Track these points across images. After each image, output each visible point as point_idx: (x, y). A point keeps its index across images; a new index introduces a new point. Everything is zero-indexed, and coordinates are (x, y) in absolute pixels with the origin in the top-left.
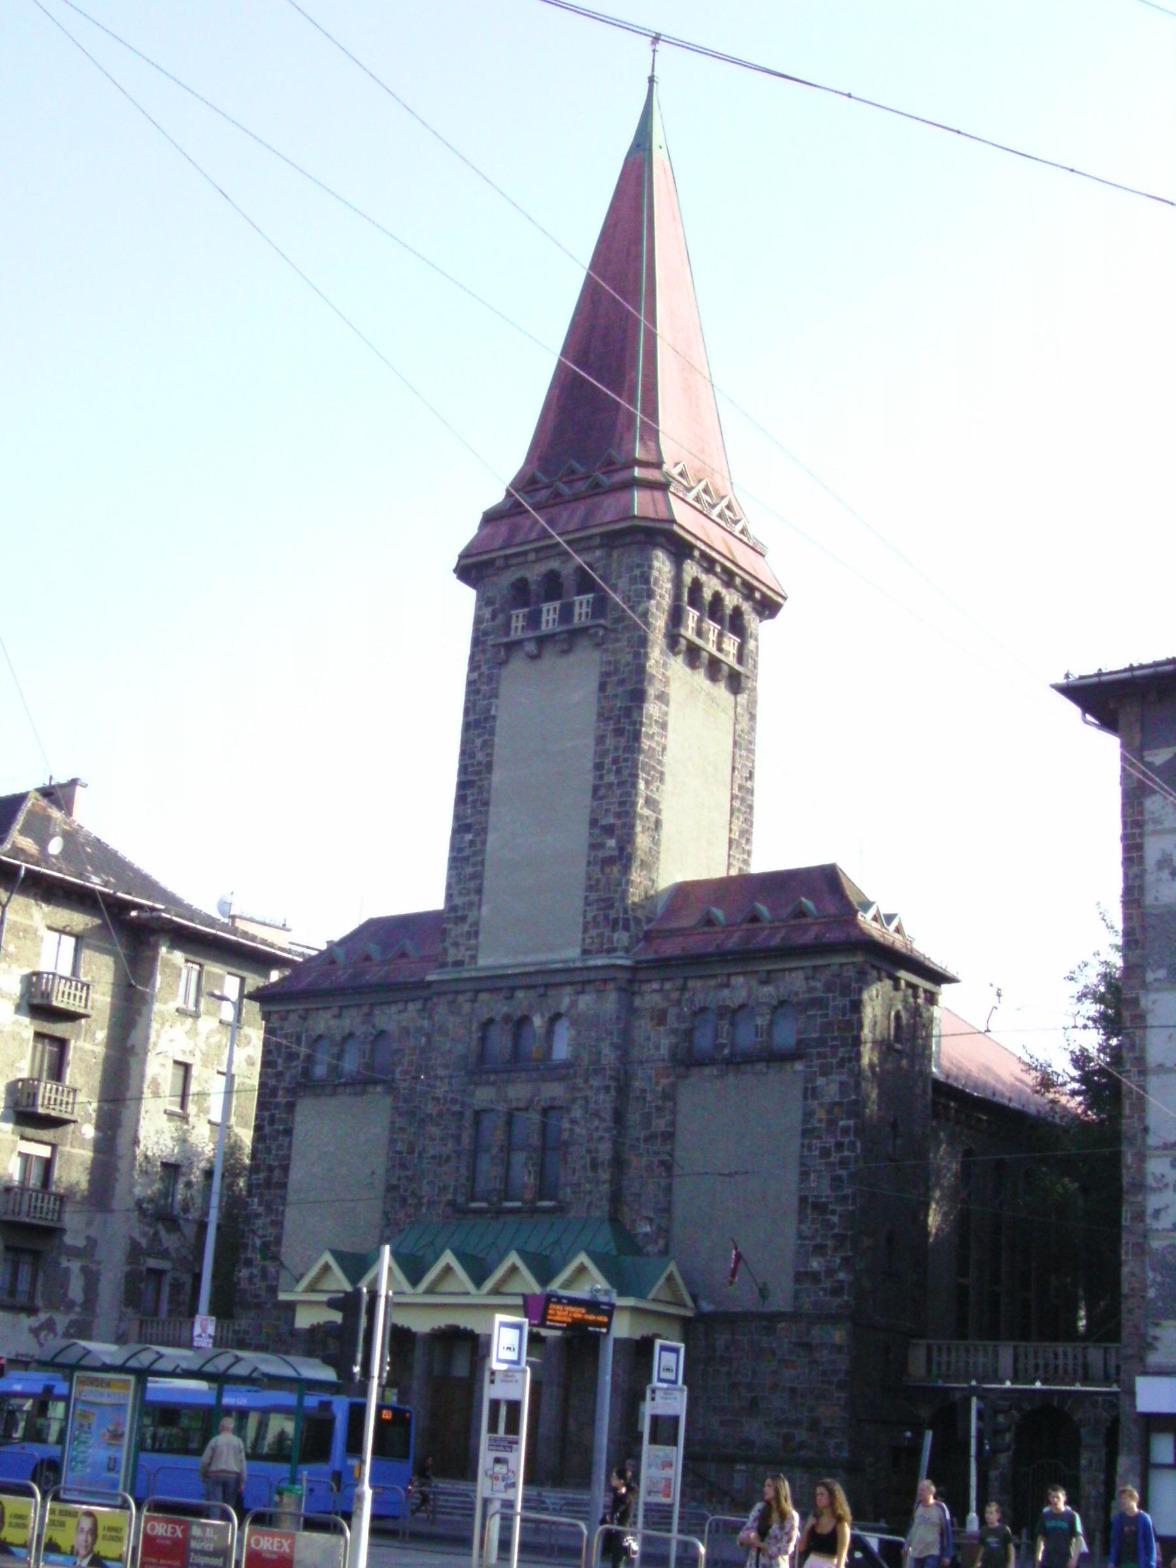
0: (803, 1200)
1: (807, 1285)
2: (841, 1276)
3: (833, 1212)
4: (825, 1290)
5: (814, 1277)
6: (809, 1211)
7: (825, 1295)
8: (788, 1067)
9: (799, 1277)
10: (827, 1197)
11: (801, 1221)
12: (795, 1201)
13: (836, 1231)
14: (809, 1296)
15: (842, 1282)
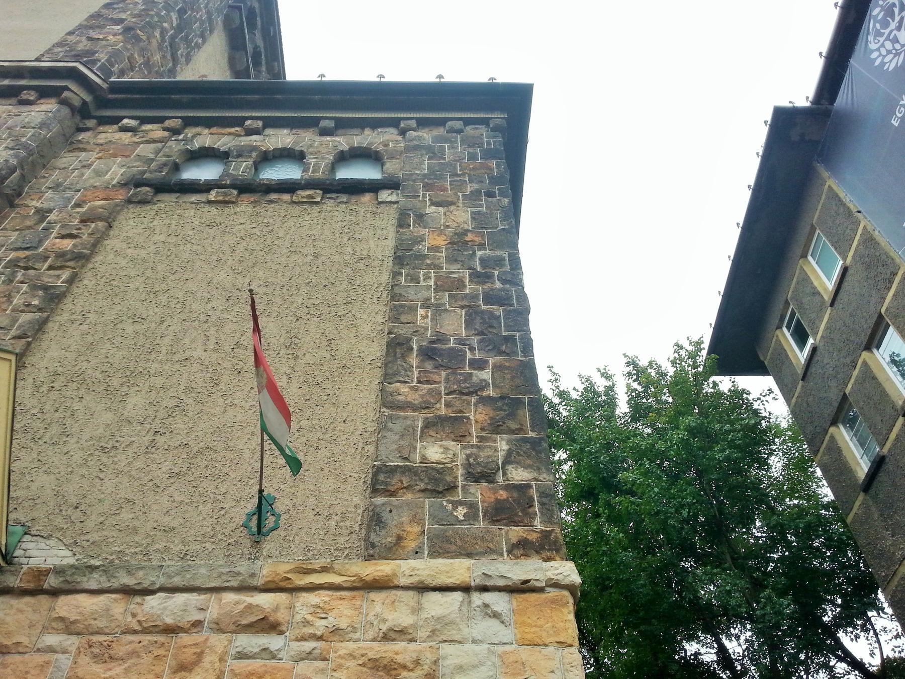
0: (397, 347)
1: (409, 496)
2: (519, 475)
3: (479, 365)
4: (472, 506)
5: (438, 483)
6: (414, 360)
7: (472, 516)
8: (367, 198)
9: (381, 481)
10: (461, 342)
11: (387, 378)
12: (376, 350)
13: (491, 392)
14: (416, 519)
15: (523, 488)
